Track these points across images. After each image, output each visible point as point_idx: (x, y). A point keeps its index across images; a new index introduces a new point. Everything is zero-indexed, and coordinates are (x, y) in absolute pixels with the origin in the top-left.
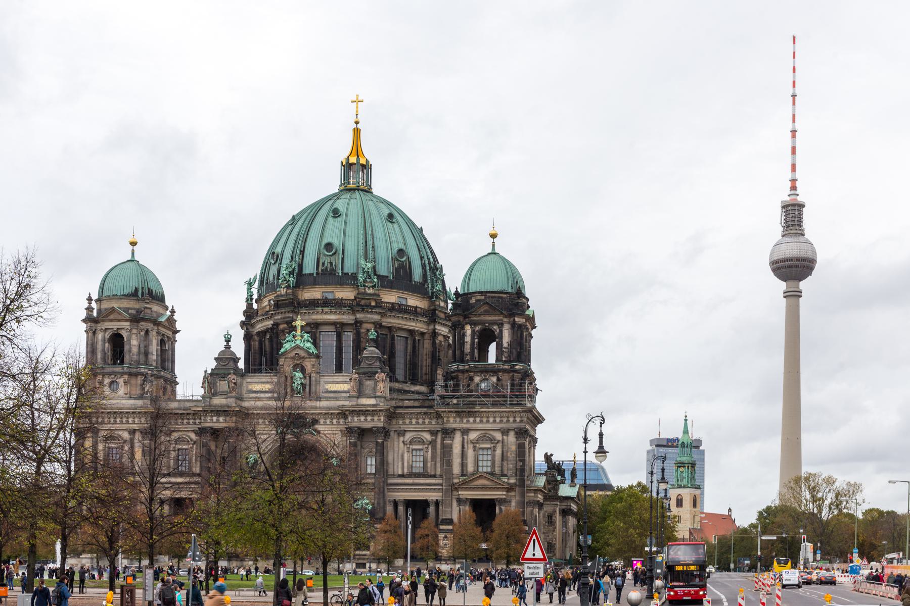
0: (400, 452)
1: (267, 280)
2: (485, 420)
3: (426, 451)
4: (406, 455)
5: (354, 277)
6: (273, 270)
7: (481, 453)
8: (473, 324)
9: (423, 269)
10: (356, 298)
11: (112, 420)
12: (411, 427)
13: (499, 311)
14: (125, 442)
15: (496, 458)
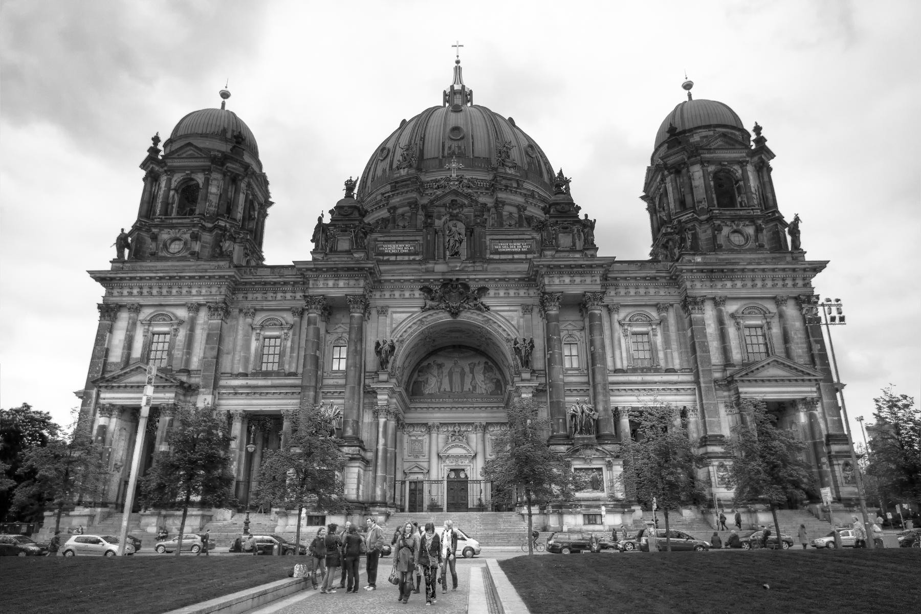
0: (616, 335)
1: (373, 178)
2: (749, 284)
3: (655, 335)
4: (623, 341)
5: (488, 160)
6: (385, 164)
7: (747, 332)
8: (702, 162)
9: (548, 173)
10: (495, 177)
11: (164, 291)
12: (629, 301)
13: (741, 143)
14: (181, 322)
15: (775, 340)
